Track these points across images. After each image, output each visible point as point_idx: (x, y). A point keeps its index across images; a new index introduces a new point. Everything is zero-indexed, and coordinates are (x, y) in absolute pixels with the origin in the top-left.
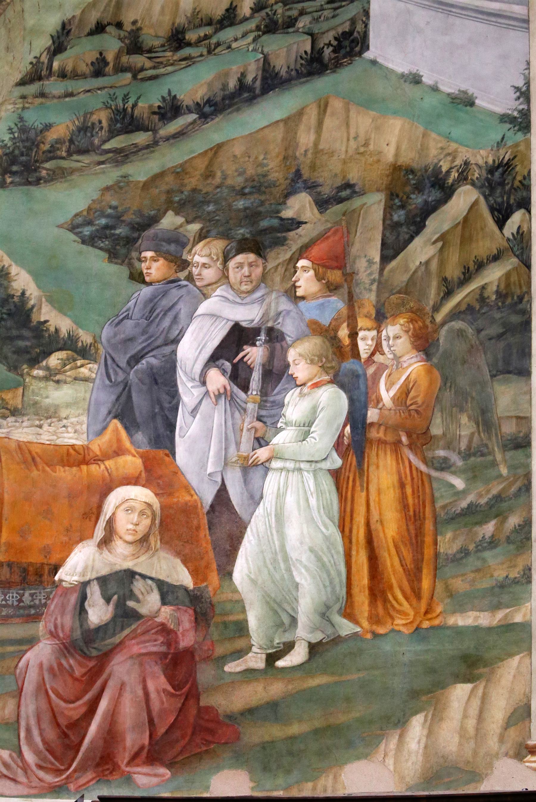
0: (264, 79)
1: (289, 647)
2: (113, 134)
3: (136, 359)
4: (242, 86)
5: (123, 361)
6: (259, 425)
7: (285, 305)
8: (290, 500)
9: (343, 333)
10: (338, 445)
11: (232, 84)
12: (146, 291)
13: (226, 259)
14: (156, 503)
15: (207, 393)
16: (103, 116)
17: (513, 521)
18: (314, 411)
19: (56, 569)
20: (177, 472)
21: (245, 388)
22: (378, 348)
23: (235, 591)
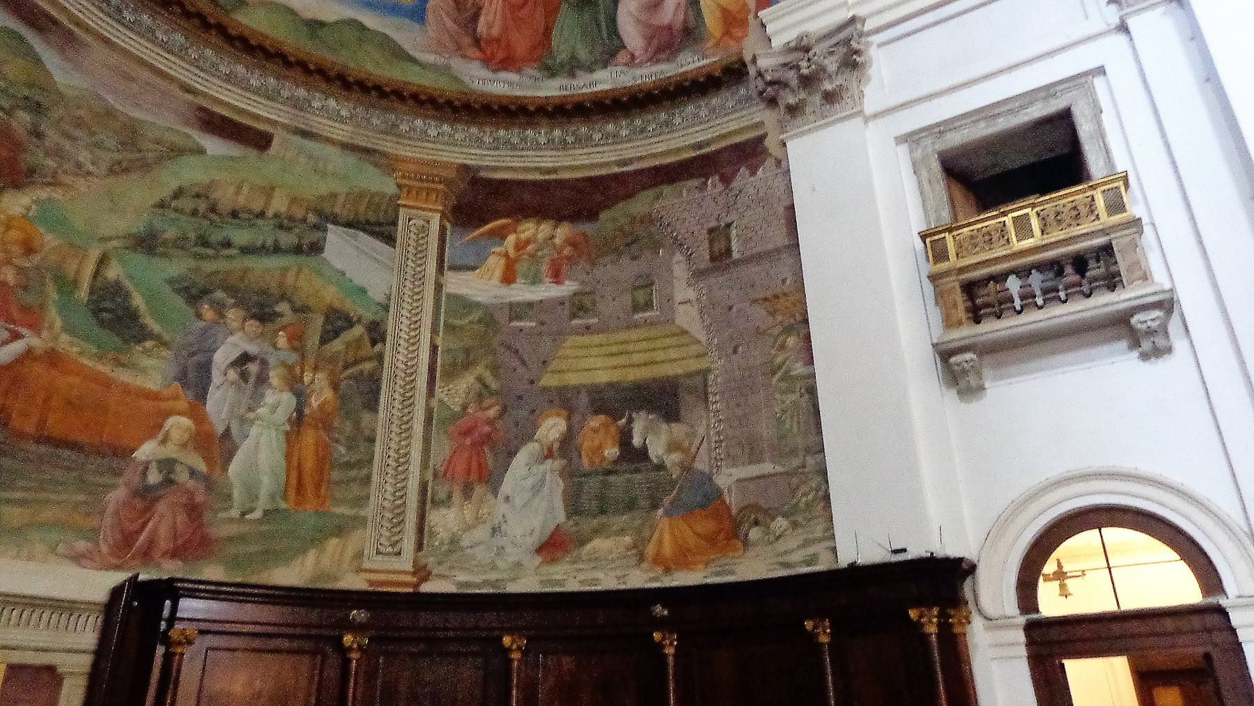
0: (275, 248)
1: (252, 510)
2: (196, 245)
3: (194, 354)
4: (263, 247)
5: (185, 353)
6: (251, 401)
7: (271, 349)
8: (263, 440)
9: (298, 370)
10: (289, 420)
11: (259, 243)
12: (201, 324)
13: (245, 320)
14: (193, 426)
15: (226, 380)
16: (192, 235)
17: (365, 471)
18: (279, 402)
19: (133, 451)
20: (205, 413)
21: (246, 381)
22: (312, 382)
23: (227, 478)
